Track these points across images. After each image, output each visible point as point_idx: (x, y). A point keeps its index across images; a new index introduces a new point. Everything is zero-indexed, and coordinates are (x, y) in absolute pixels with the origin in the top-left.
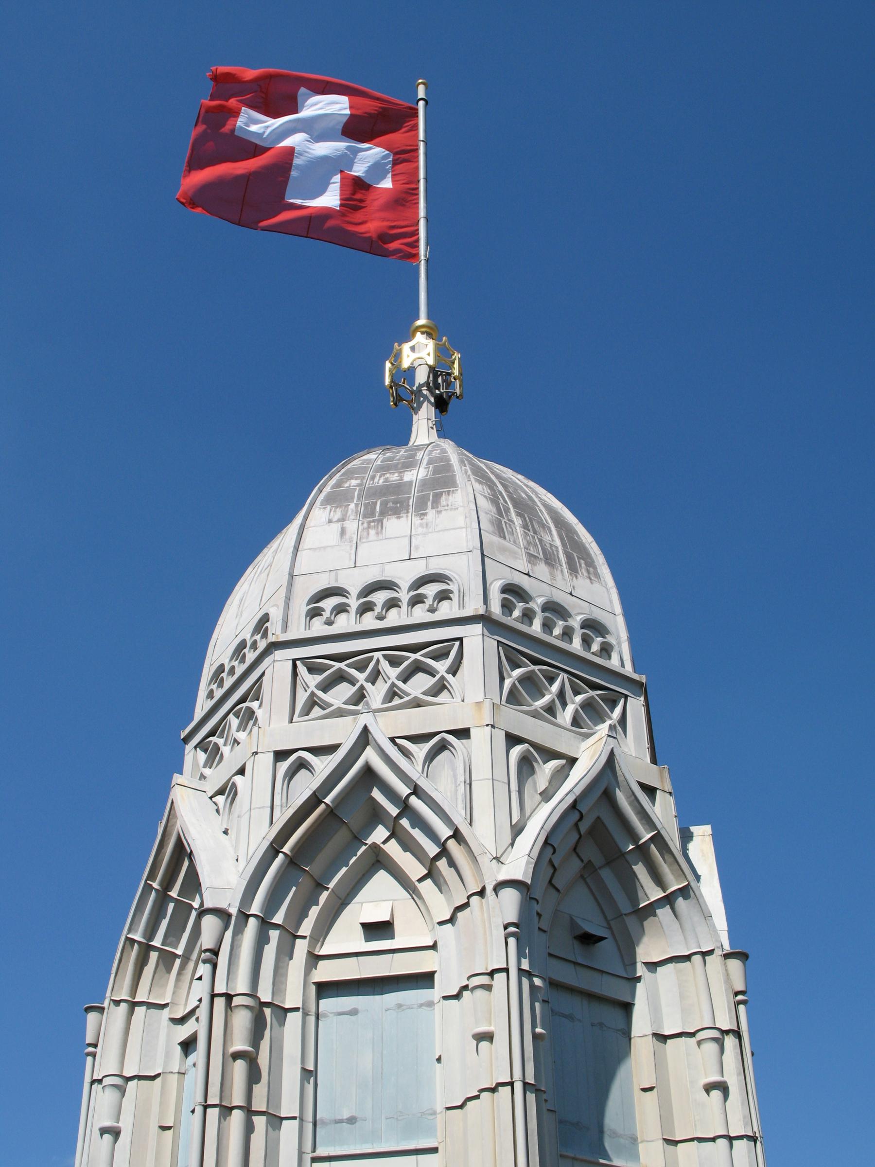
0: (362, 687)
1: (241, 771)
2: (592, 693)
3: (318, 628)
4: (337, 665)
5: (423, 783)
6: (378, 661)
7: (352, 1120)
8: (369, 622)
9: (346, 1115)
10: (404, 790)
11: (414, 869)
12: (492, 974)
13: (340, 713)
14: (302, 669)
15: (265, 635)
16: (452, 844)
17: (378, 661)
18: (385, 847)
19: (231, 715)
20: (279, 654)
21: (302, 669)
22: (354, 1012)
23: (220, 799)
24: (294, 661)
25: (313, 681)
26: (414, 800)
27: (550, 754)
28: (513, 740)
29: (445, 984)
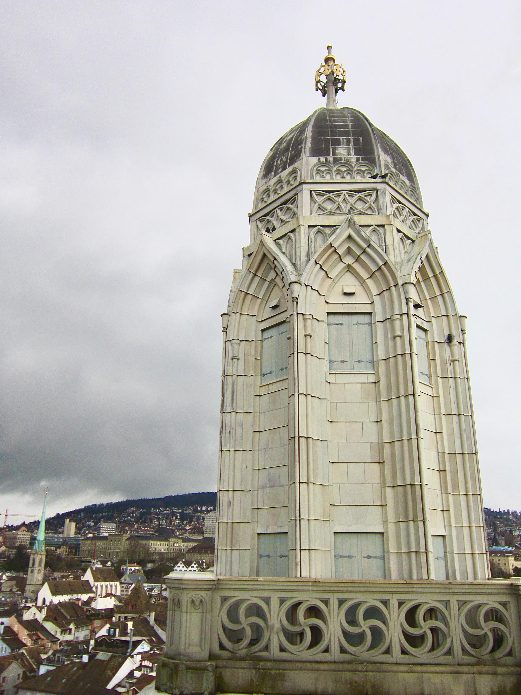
0: (339, 204)
1: (293, 231)
2: (415, 217)
3: (318, 179)
4: (329, 195)
5: (372, 243)
6: (345, 195)
7: (342, 361)
8: (338, 179)
9: (340, 360)
10: (364, 246)
11: (364, 275)
12: (401, 315)
13: (331, 214)
14: (314, 194)
15: (295, 178)
16: (383, 267)
17: (345, 195)
18: (353, 266)
19: (277, 209)
20: (304, 186)
21: (314, 194)
22: (341, 324)
23: (280, 241)
24: (311, 191)
25: (319, 199)
26: (368, 250)
27: (409, 238)
28: (399, 231)
29: (379, 316)
